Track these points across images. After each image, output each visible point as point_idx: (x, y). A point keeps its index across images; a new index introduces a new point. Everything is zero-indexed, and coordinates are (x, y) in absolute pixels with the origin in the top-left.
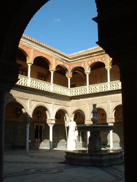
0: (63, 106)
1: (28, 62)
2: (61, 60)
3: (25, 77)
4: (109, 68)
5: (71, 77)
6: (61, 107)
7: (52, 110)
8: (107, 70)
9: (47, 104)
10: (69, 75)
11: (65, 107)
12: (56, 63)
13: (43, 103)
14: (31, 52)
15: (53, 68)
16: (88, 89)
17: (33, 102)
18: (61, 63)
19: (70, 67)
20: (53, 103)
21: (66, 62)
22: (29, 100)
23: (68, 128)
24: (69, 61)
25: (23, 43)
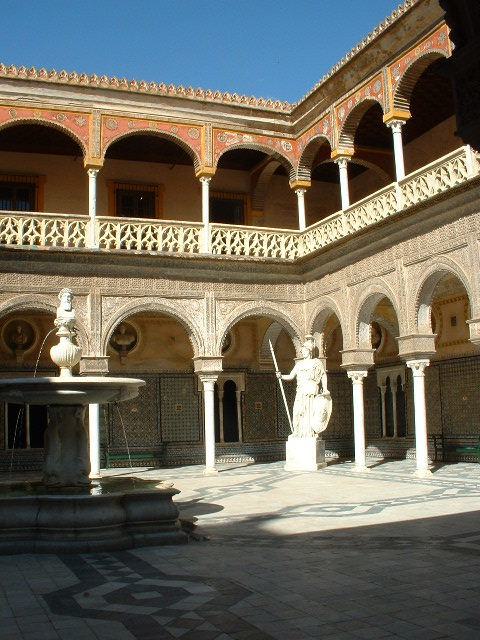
0: (261, 303)
1: (85, 164)
2: (242, 129)
3: (69, 217)
4: (395, 121)
5: (309, 184)
6: (252, 305)
7: (208, 321)
8: (390, 129)
9: (178, 301)
10: (300, 179)
11: (274, 306)
12: (216, 144)
13: (157, 300)
14: (91, 126)
15: (206, 163)
16: (352, 218)
17: (107, 303)
18: (248, 141)
19: (291, 150)
20: (210, 295)
21: (272, 133)
22: (89, 298)
23: (291, 387)
24: (289, 124)
25: (51, 101)
